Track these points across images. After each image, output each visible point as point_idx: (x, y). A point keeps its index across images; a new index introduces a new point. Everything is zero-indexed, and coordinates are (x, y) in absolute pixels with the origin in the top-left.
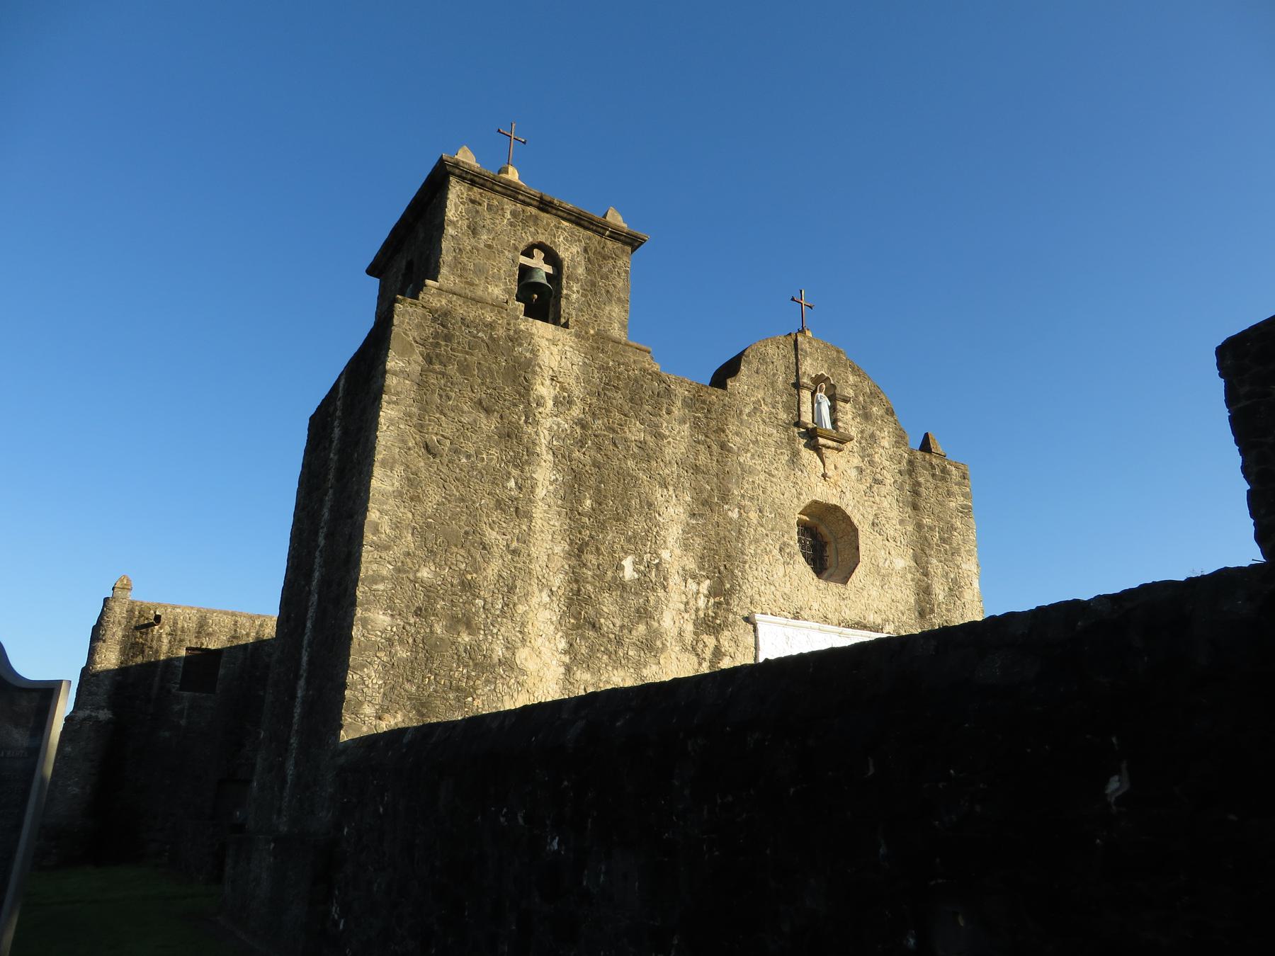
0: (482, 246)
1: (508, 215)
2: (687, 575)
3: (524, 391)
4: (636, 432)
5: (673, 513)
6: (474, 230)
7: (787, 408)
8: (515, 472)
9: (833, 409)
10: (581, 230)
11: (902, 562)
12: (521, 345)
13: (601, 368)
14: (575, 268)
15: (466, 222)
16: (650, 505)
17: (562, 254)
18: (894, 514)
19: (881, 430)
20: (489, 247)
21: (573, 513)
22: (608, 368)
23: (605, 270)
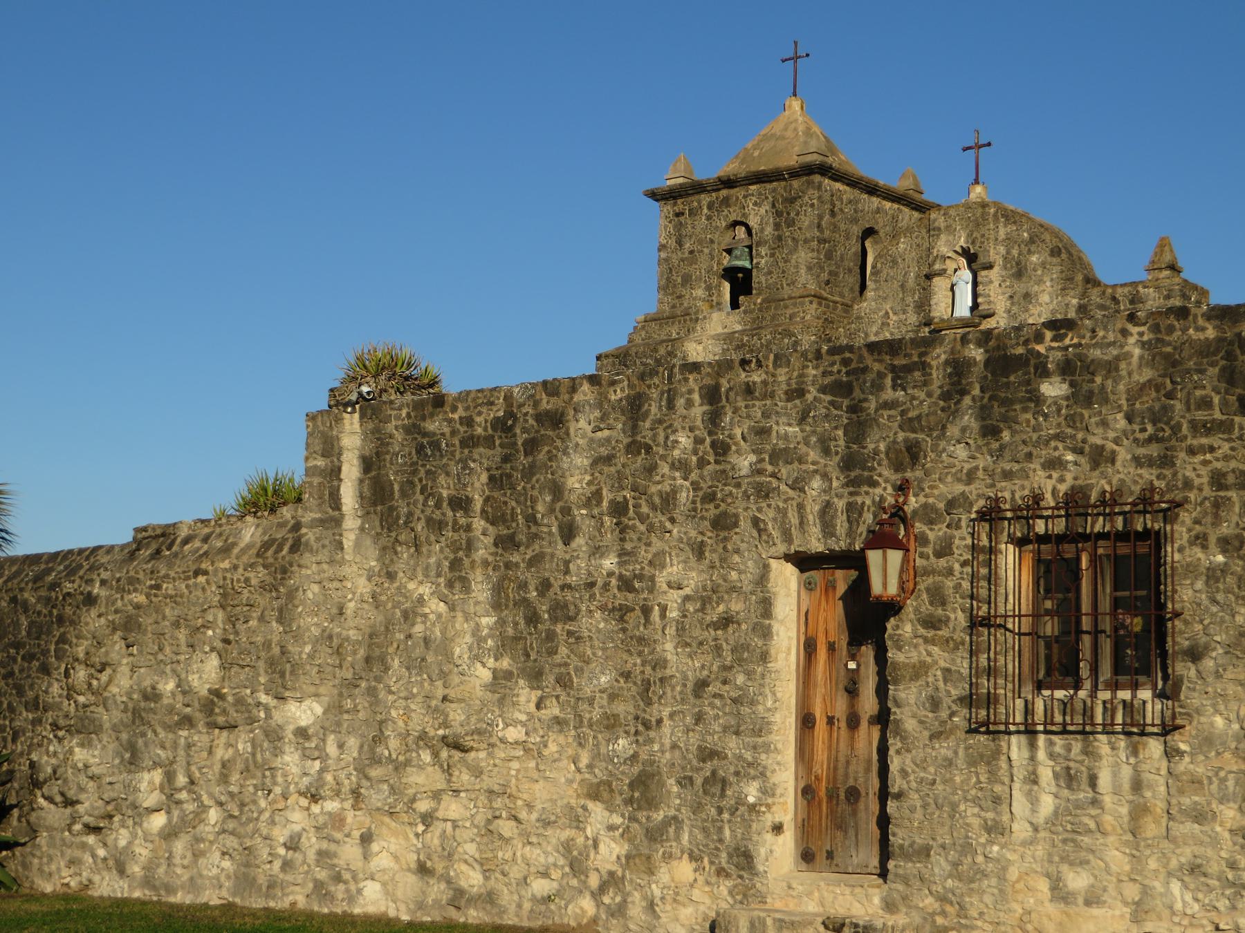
0: (686, 255)
1: (705, 211)
6: (680, 243)
10: (768, 186)
12: (675, 356)
13: (738, 348)
14: (762, 230)
15: (674, 239)
17: (753, 222)
19: (1040, 282)
20: (691, 252)
22: (744, 345)
23: (792, 215)
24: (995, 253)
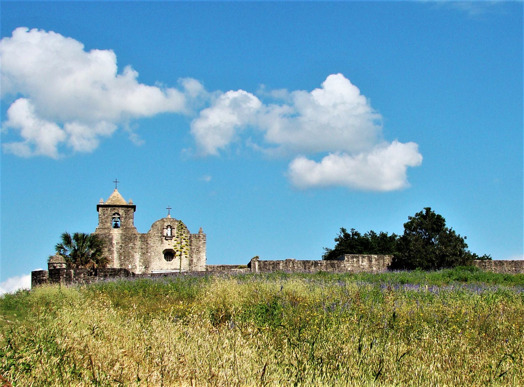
2: (140, 266)
3: (111, 244)
4: (131, 245)
5: (137, 256)
6: (104, 215)
7: (161, 233)
9: (171, 231)
17: (120, 213)
21: (120, 259)
24: (176, 227)
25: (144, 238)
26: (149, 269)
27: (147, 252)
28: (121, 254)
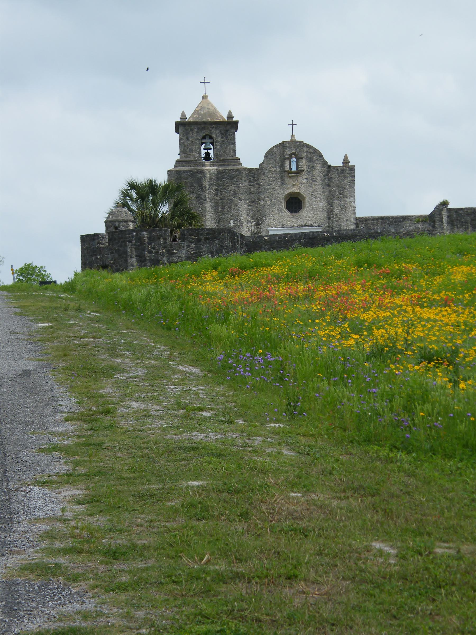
3: (201, 186)
4: (232, 188)
5: (243, 207)
8: (201, 206)
11: (322, 204)
16: (237, 206)
17: (214, 136)
18: (320, 191)
20: (192, 142)
24: (304, 155)
25: (253, 174)
26: (262, 226)
27: (259, 199)
28: (217, 203)
